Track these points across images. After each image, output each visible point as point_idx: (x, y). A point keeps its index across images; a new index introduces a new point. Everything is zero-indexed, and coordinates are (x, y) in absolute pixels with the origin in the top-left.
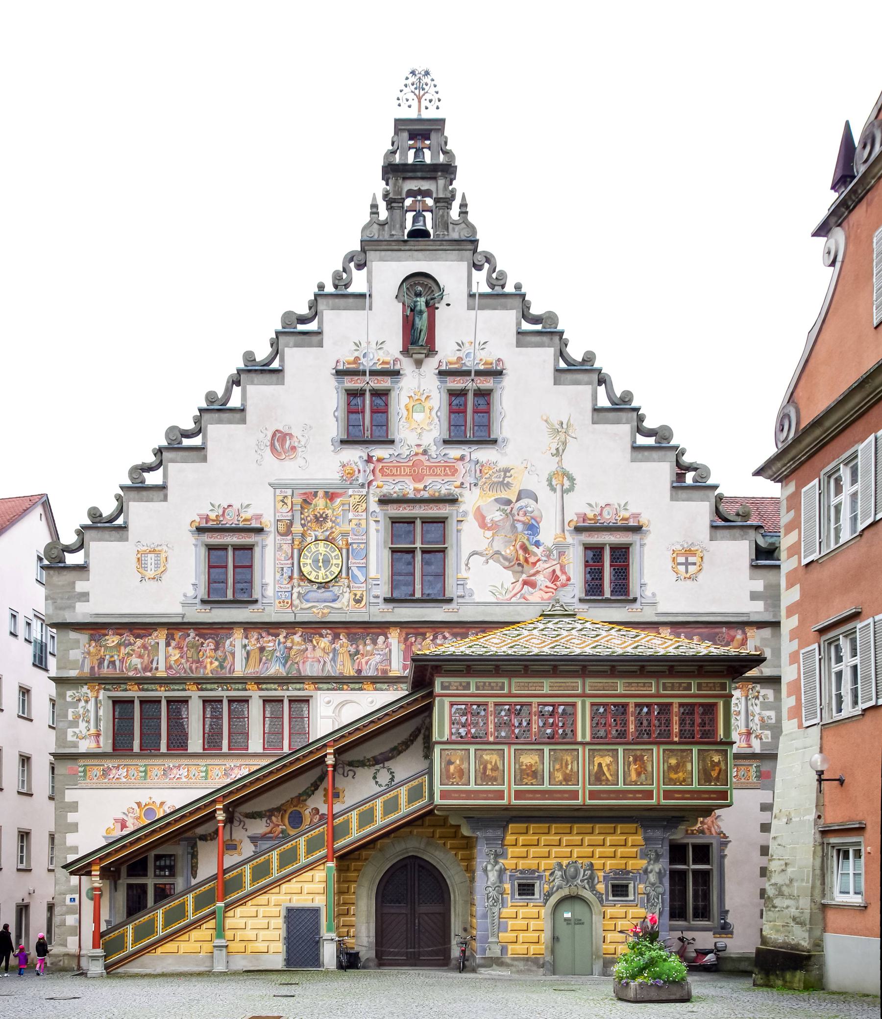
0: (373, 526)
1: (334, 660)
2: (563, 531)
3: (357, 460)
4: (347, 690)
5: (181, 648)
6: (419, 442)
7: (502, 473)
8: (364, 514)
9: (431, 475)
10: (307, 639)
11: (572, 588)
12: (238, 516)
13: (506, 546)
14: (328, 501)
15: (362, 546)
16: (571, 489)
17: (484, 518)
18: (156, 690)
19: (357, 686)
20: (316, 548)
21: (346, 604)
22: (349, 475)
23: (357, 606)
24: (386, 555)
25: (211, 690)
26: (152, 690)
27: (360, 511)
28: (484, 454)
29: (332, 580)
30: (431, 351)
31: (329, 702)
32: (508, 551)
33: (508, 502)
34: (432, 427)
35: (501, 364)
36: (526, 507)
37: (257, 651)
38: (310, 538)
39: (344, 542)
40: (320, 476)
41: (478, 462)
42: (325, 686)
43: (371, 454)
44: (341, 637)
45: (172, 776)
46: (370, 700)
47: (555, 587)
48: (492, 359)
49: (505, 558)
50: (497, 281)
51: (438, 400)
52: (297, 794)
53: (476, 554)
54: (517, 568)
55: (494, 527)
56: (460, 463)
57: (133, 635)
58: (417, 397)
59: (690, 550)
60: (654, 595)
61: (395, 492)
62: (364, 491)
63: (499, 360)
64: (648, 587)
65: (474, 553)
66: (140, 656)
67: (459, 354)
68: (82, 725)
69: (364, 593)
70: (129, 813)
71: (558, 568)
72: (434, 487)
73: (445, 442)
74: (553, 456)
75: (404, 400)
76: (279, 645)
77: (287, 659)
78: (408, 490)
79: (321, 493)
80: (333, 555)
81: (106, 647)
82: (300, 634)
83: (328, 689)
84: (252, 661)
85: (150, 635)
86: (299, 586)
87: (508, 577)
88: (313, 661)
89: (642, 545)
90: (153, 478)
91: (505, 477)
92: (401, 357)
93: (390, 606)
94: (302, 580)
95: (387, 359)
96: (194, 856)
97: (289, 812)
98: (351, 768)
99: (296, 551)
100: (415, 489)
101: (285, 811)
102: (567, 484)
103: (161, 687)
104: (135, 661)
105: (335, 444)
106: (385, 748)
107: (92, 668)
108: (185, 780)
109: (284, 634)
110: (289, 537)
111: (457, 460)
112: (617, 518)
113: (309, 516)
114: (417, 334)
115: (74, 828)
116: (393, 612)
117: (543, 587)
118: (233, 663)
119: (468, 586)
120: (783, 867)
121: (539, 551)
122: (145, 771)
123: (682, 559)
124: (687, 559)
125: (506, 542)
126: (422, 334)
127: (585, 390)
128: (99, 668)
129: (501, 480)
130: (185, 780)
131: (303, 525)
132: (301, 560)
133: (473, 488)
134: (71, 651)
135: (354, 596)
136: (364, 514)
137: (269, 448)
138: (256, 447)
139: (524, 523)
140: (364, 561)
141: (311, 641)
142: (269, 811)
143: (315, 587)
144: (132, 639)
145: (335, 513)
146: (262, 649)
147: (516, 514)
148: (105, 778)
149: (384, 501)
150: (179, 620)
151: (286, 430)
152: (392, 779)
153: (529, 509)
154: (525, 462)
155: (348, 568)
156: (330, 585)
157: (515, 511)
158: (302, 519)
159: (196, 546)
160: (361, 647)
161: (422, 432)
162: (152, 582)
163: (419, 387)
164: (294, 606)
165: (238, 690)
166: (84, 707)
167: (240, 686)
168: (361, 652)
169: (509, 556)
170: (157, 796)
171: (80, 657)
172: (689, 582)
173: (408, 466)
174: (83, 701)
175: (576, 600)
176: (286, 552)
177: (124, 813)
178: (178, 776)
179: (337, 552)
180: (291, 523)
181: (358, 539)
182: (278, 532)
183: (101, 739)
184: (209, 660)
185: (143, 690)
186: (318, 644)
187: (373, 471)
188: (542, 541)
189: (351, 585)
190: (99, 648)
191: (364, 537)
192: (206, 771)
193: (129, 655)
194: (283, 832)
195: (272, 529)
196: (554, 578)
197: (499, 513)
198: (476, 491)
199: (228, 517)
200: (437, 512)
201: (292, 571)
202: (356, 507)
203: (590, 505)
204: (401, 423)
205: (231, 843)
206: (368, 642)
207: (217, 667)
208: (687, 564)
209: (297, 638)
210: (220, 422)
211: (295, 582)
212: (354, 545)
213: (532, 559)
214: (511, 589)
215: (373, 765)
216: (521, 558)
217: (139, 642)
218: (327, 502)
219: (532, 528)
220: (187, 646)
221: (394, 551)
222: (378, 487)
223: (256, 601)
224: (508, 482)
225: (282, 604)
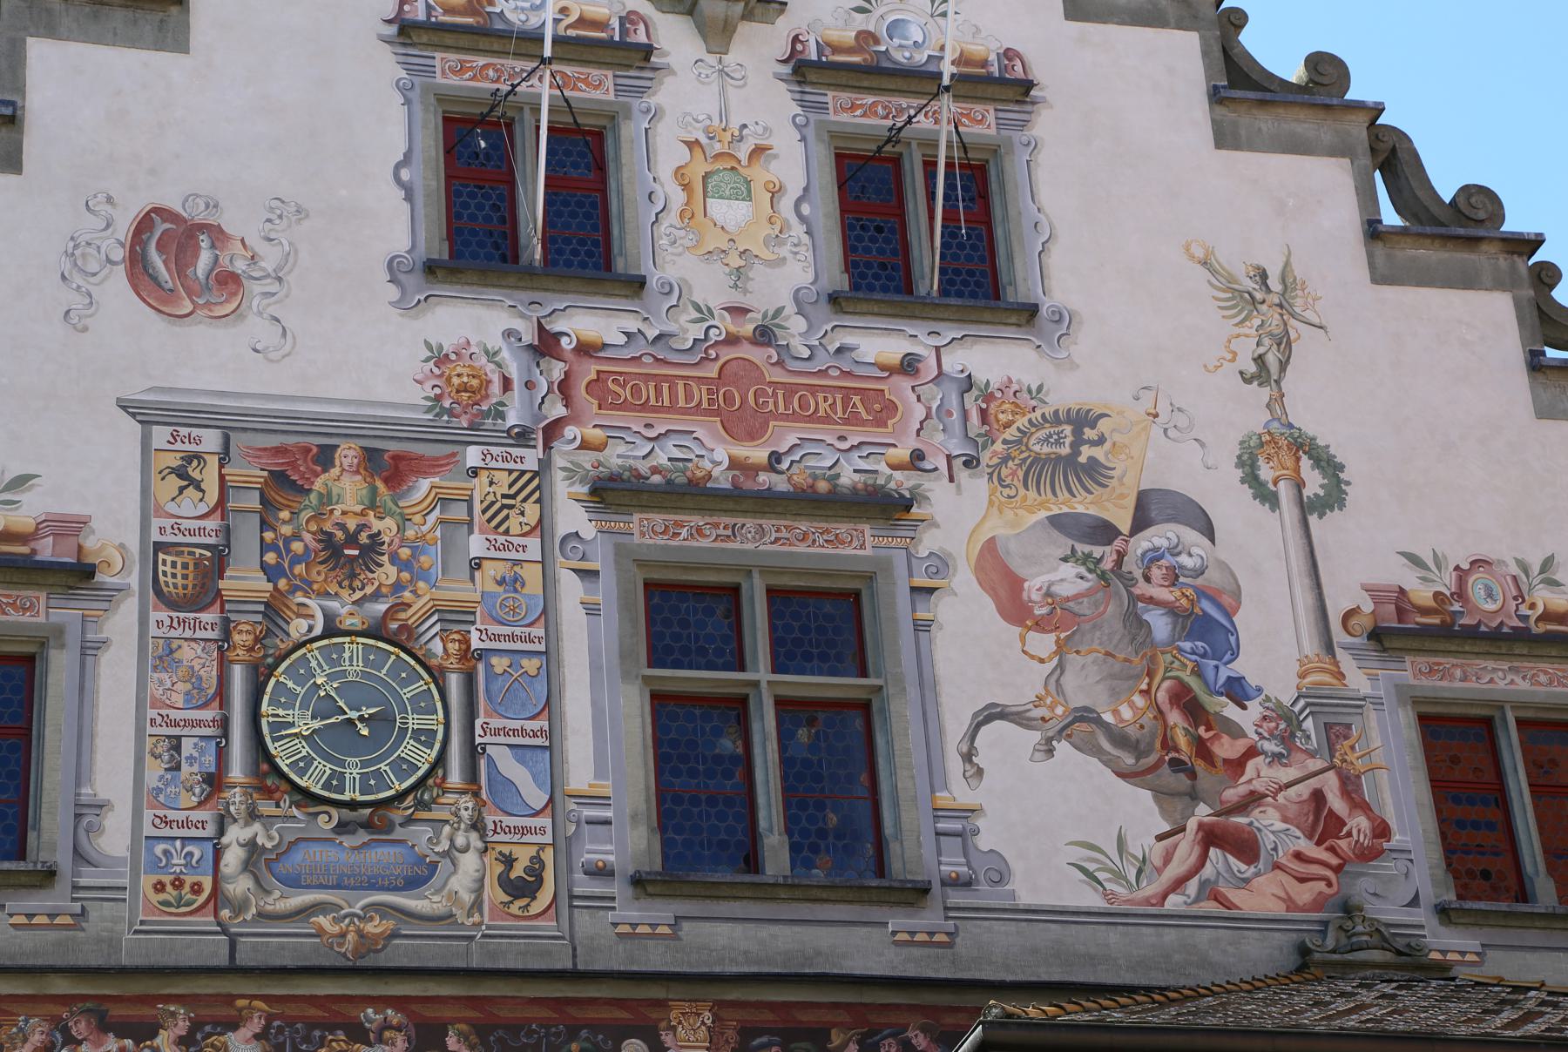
0: (571, 590)
2: (1329, 647)
6: (738, 299)
7: (1068, 429)
8: (533, 543)
9: (793, 417)
11: (1402, 865)
13: (1115, 694)
14: (380, 485)
15: (530, 665)
16: (1334, 498)
17: (1015, 583)
20: (332, 663)
21: (467, 898)
23: (515, 909)
27: (515, 529)
29: (401, 796)
32: (1127, 713)
33: (1104, 532)
34: (784, 251)
35: (1019, 68)
36: (1174, 551)
38: (303, 625)
39: (453, 647)
41: (968, 383)
43: (557, 326)
47: (1335, 861)
48: (987, 46)
49: (1120, 739)
53: (1003, 716)
54: (1167, 776)
56: (904, 383)
58: (718, 148)
61: (655, 470)
62: (531, 458)
63: (1009, 54)
65: (991, 714)
67: (860, 23)
69: (548, 856)
71: (1330, 783)
72: (811, 462)
74: (1248, 380)
75: (670, 155)
78: (707, 465)
79: (347, 454)
80: (407, 693)
82: (256, 1025)
86: (253, 815)
91: (1078, 442)
93: (661, 912)
94: (268, 793)
99: (238, 674)
100: (734, 464)
102: (1314, 483)
105: (402, 277)
109: (182, 1027)
110: (208, 617)
111: (892, 370)
112: (1524, 610)
113: (297, 537)
116: (674, 937)
117: (1282, 857)
119: (984, 842)
121: (1247, 718)
125: (1112, 676)
129: (1065, 450)
131: (272, 573)
132: (265, 707)
133: (963, 475)
135: (499, 868)
136: (533, 543)
137: (120, 272)
138: (67, 266)
139: (1171, 610)
140: (542, 723)
143: (326, 822)
145: (410, 533)
147: (1138, 574)
151: (198, 214)
153: (1184, 560)
154: (1151, 395)
155: (473, 753)
156: (397, 815)
157: (1131, 565)
158: (264, 547)
161: (750, 266)
163: (724, 114)
164: (228, 902)
169: (1133, 732)
173: (700, 380)
175: (1422, 916)
176: (192, 676)
179: (424, 683)
180: (219, 559)
181: (512, 638)
182: (158, 592)
187: (564, 388)
188: (1252, 680)
189: (489, 820)
191: (538, 631)
195: (134, 580)
196: (1323, 824)
197: (1069, 570)
198: (976, 486)
200: (830, 551)
201: (222, 755)
202: (497, 516)
203: (1414, 560)
204: (663, 228)
211: (236, 798)
212: (494, 660)
213: (1226, 749)
214: (1157, 861)
216: (1182, 741)
218: (374, 491)
224: (1092, 460)
225: (170, 894)
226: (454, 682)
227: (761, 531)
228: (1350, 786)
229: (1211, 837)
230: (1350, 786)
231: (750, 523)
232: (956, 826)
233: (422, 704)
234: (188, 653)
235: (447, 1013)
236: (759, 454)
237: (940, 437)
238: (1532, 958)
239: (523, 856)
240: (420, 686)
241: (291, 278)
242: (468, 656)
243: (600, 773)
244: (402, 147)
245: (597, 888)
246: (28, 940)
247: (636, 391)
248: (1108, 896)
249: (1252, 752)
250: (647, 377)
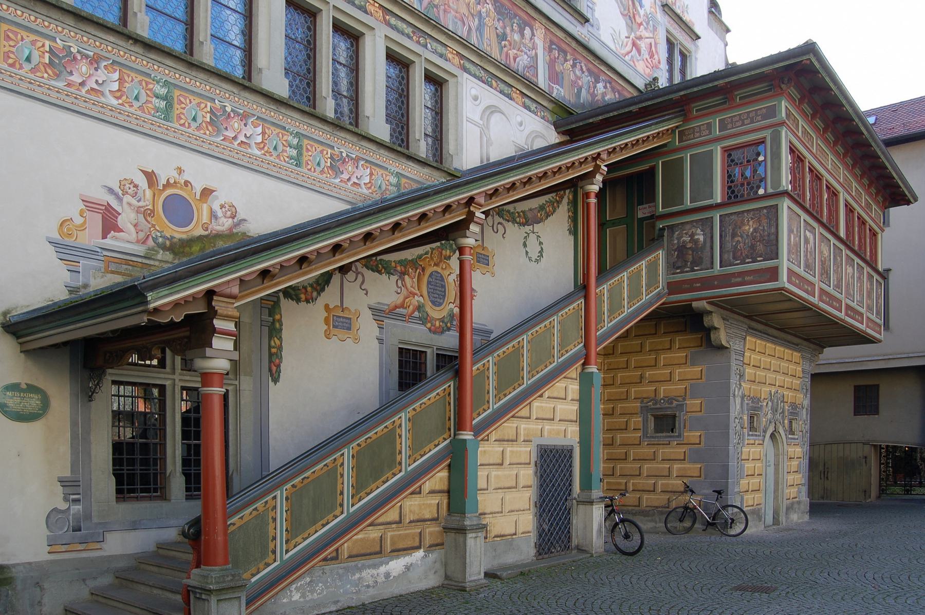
4: (495, 89)
45: (230, 134)
70: (125, 193)
88: (456, 17)
98: (501, 220)
101: (423, 269)
148: (58, 76)
168: (509, 38)
177: (111, 191)
178: (241, 138)
194: (419, 308)
205: (341, 314)
206: (515, 27)
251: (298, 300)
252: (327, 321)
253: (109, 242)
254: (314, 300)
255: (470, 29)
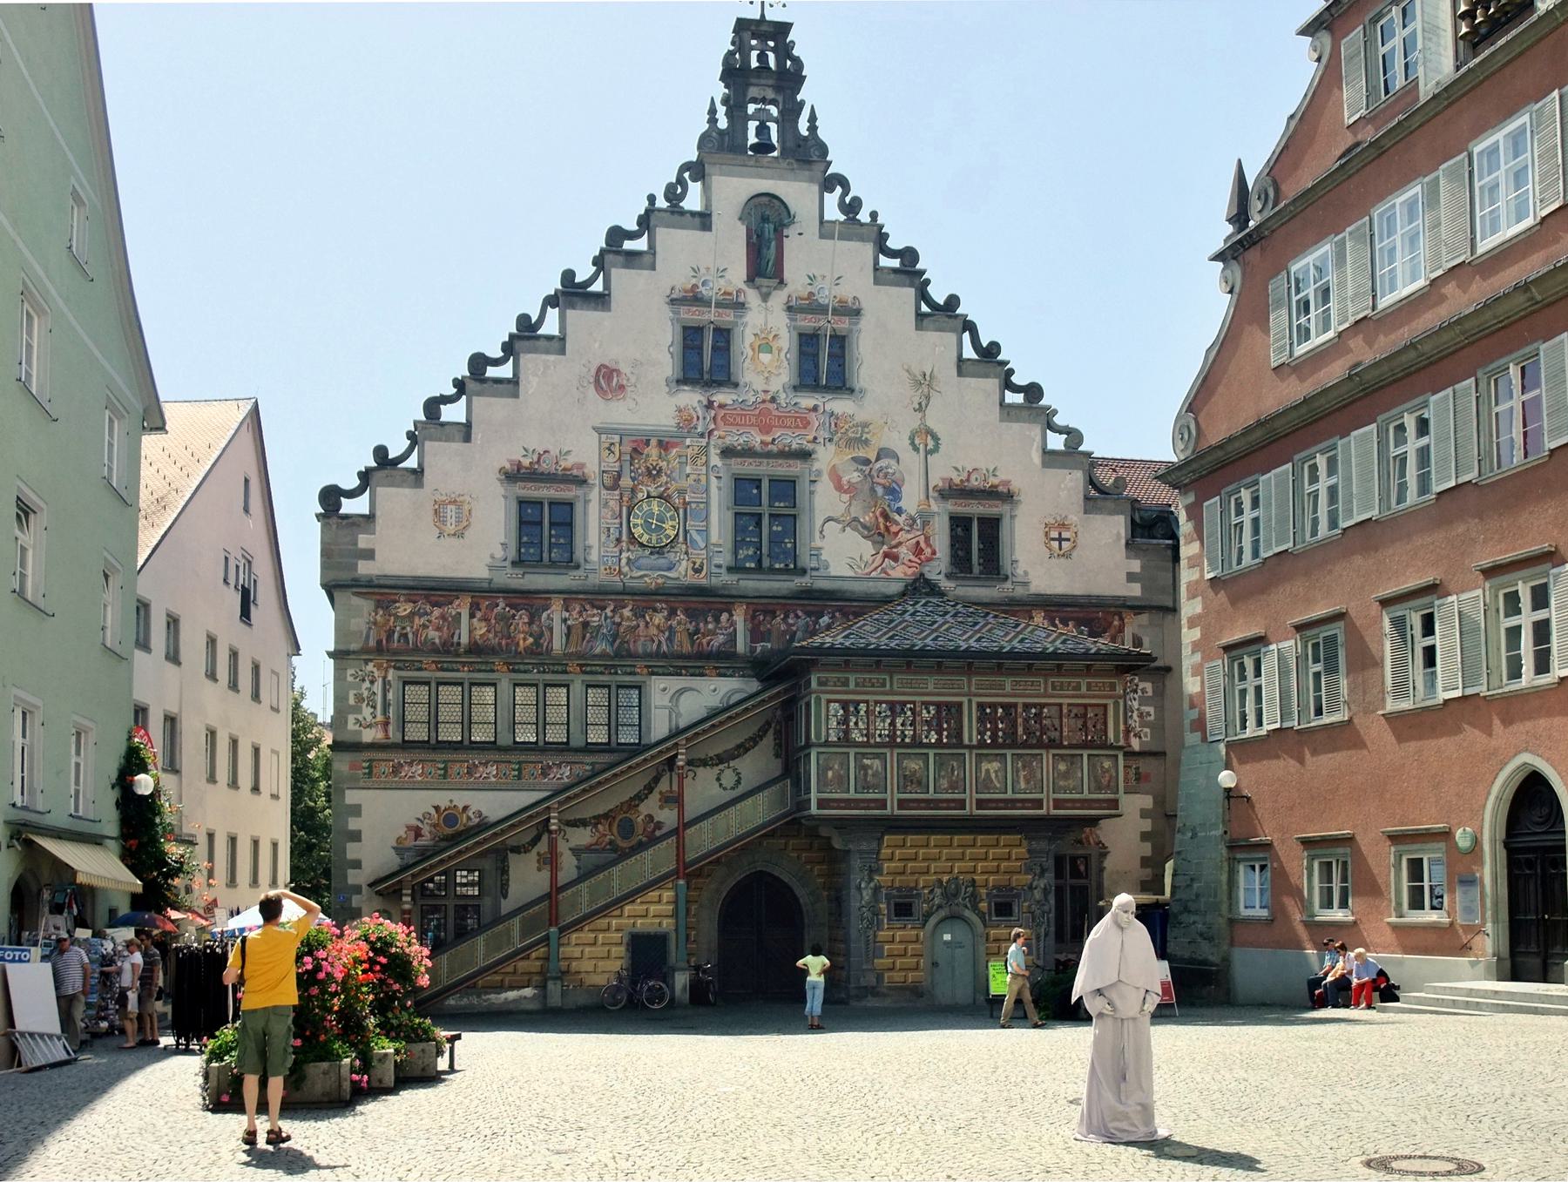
0: (714, 481)
1: (670, 639)
2: (928, 497)
3: (696, 404)
5: (485, 619)
6: (766, 388)
8: (704, 468)
9: (781, 427)
10: (639, 613)
12: (557, 463)
15: (702, 506)
16: (936, 449)
18: (458, 670)
19: (697, 671)
21: (684, 573)
22: (686, 424)
24: (729, 517)
25: (525, 672)
26: (453, 670)
28: (840, 405)
30: (782, 282)
31: (664, 689)
32: (867, 519)
33: (867, 462)
34: (781, 371)
37: (580, 626)
40: (652, 421)
42: (660, 670)
43: (713, 399)
44: (679, 613)
45: (478, 775)
46: (712, 687)
49: (864, 527)
50: (851, 208)
51: (786, 341)
52: (627, 798)
55: (851, 490)
56: (814, 414)
57: (430, 602)
58: (763, 335)
59: (1064, 525)
60: (1026, 573)
62: (704, 442)
64: (1020, 564)
66: (438, 629)
67: (810, 289)
68: (367, 711)
72: (784, 441)
73: (795, 388)
75: (749, 338)
76: (605, 620)
77: (615, 636)
79: (653, 442)
80: (668, 515)
81: (397, 617)
82: (630, 607)
83: (664, 674)
84: (573, 638)
85: (451, 603)
86: (629, 550)
87: (867, 548)
89: (1013, 517)
90: (453, 413)
92: (744, 287)
93: (735, 577)
94: (632, 544)
95: (730, 289)
96: (504, 871)
97: (617, 822)
98: (691, 768)
99: (624, 509)
100: (762, 442)
101: (614, 818)
102: (931, 444)
103: (463, 667)
104: (433, 634)
106: (730, 745)
107: (379, 642)
108: (493, 779)
109: (612, 607)
110: (617, 492)
111: (810, 410)
114: (764, 263)
115: (356, 836)
118: (551, 640)
119: (823, 558)
120: (1189, 883)
121: (900, 519)
122: (445, 769)
123: (1055, 534)
124: (1060, 534)
126: (770, 264)
127: (951, 338)
128: (387, 641)
129: (859, 435)
130: (493, 779)
131: (633, 479)
133: (828, 444)
134: (353, 621)
137: (592, 387)
139: (884, 487)
141: (644, 617)
142: (594, 817)
143: (647, 552)
144: (428, 608)
146: (586, 624)
148: (395, 776)
149: (727, 452)
150: (485, 585)
151: (612, 365)
152: (738, 782)
153: (890, 470)
155: (686, 532)
156: (666, 550)
157: (874, 473)
158: (631, 471)
159: (505, 497)
160: (702, 625)
162: (452, 539)
165: (557, 672)
166: (369, 689)
167: (560, 668)
169: (868, 525)
170: (460, 798)
171: (364, 629)
172: (1062, 560)
174: (368, 682)
175: (941, 577)
176: (613, 510)
177: (419, 819)
180: (619, 475)
183: (391, 728)
184: (522, 636)
185: (442, 669)
186: (651, 619)
187: (714, 418)
188: (904, 508)
190: (387, 617)
192: (519, 770)
193: (425, 626)
194: (611, 842)
196: (918, 550)
197: (856, 474)
198: (831, 447)
199: (544, 465)
201: (620, 533)
202: (694, 463)
204: (745, 365)
206: (710, 619)
207: (532, 644)
208: (1060, 540)
209: (627, 612)
210: (535, 351)
211: (624, 544)
213: (894, 529)
215: (717, 765)
216: (882, 526)
217: (437, 612)
219: (894, 492)
220: (495, 619)
221: (736, 514)
222: (719, 437)
223: (578, 567)
226: (681, 511)
227: (768, 464)
228: (927, 539)
229: (886, 555)
230: (927, 539)
231: (765, 461)
232: (816, 553)
233: (672, 518)
234: (612, 503)
235: (677, 605)
236: (770, 439)
237: (822, 432)
238: (969, 589)
239: (698, 562)
240: (672, 513)
241: (638, 386)
242: (685, 504)
243: (720, 538)
244: (671, 340)
245: (718, 571)
246: (574, 583)
247: (735, 419)
248: (855, 572)
249: (901, 530)
250: (738, 415)
251: (519, 853)
252: (538, 861)
253: (418, 843)
254: (529, 851)
255: (660, 642)
